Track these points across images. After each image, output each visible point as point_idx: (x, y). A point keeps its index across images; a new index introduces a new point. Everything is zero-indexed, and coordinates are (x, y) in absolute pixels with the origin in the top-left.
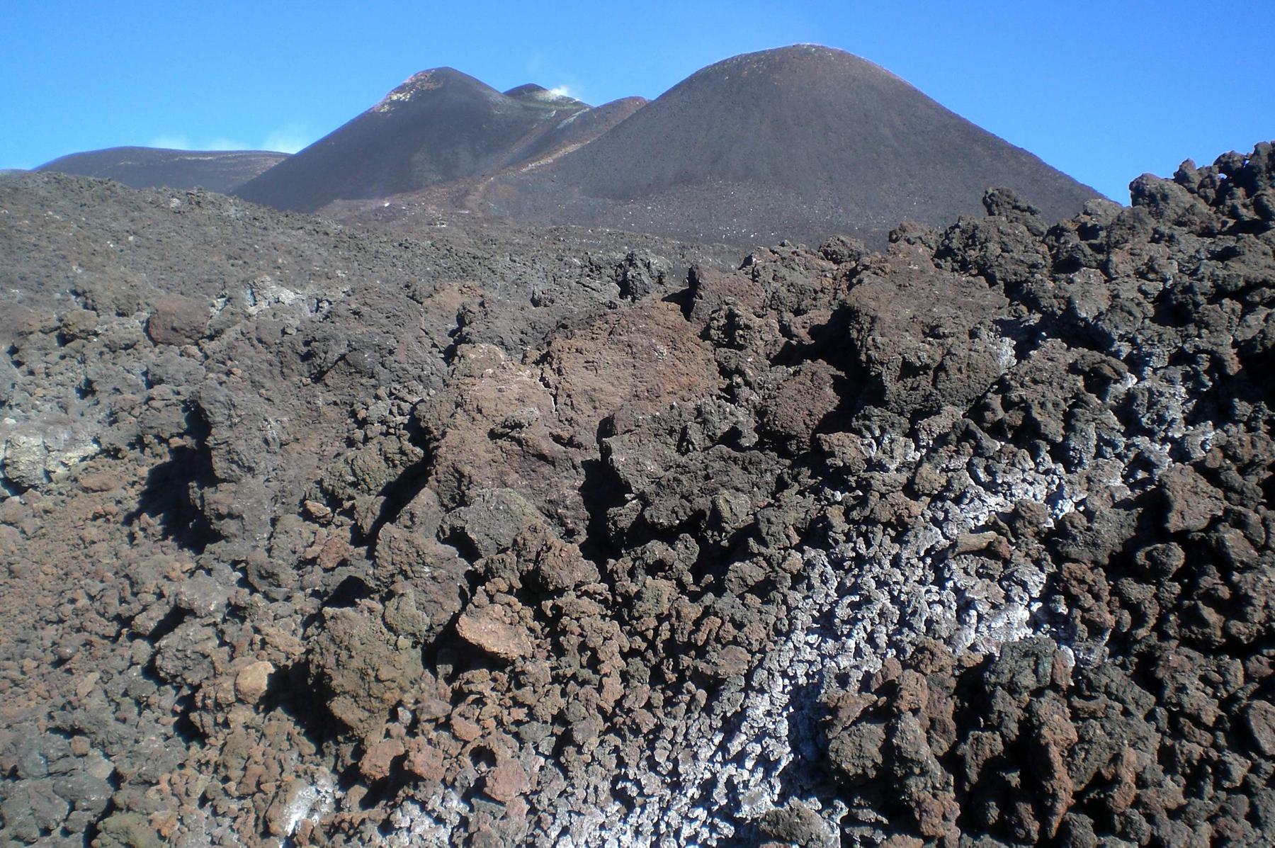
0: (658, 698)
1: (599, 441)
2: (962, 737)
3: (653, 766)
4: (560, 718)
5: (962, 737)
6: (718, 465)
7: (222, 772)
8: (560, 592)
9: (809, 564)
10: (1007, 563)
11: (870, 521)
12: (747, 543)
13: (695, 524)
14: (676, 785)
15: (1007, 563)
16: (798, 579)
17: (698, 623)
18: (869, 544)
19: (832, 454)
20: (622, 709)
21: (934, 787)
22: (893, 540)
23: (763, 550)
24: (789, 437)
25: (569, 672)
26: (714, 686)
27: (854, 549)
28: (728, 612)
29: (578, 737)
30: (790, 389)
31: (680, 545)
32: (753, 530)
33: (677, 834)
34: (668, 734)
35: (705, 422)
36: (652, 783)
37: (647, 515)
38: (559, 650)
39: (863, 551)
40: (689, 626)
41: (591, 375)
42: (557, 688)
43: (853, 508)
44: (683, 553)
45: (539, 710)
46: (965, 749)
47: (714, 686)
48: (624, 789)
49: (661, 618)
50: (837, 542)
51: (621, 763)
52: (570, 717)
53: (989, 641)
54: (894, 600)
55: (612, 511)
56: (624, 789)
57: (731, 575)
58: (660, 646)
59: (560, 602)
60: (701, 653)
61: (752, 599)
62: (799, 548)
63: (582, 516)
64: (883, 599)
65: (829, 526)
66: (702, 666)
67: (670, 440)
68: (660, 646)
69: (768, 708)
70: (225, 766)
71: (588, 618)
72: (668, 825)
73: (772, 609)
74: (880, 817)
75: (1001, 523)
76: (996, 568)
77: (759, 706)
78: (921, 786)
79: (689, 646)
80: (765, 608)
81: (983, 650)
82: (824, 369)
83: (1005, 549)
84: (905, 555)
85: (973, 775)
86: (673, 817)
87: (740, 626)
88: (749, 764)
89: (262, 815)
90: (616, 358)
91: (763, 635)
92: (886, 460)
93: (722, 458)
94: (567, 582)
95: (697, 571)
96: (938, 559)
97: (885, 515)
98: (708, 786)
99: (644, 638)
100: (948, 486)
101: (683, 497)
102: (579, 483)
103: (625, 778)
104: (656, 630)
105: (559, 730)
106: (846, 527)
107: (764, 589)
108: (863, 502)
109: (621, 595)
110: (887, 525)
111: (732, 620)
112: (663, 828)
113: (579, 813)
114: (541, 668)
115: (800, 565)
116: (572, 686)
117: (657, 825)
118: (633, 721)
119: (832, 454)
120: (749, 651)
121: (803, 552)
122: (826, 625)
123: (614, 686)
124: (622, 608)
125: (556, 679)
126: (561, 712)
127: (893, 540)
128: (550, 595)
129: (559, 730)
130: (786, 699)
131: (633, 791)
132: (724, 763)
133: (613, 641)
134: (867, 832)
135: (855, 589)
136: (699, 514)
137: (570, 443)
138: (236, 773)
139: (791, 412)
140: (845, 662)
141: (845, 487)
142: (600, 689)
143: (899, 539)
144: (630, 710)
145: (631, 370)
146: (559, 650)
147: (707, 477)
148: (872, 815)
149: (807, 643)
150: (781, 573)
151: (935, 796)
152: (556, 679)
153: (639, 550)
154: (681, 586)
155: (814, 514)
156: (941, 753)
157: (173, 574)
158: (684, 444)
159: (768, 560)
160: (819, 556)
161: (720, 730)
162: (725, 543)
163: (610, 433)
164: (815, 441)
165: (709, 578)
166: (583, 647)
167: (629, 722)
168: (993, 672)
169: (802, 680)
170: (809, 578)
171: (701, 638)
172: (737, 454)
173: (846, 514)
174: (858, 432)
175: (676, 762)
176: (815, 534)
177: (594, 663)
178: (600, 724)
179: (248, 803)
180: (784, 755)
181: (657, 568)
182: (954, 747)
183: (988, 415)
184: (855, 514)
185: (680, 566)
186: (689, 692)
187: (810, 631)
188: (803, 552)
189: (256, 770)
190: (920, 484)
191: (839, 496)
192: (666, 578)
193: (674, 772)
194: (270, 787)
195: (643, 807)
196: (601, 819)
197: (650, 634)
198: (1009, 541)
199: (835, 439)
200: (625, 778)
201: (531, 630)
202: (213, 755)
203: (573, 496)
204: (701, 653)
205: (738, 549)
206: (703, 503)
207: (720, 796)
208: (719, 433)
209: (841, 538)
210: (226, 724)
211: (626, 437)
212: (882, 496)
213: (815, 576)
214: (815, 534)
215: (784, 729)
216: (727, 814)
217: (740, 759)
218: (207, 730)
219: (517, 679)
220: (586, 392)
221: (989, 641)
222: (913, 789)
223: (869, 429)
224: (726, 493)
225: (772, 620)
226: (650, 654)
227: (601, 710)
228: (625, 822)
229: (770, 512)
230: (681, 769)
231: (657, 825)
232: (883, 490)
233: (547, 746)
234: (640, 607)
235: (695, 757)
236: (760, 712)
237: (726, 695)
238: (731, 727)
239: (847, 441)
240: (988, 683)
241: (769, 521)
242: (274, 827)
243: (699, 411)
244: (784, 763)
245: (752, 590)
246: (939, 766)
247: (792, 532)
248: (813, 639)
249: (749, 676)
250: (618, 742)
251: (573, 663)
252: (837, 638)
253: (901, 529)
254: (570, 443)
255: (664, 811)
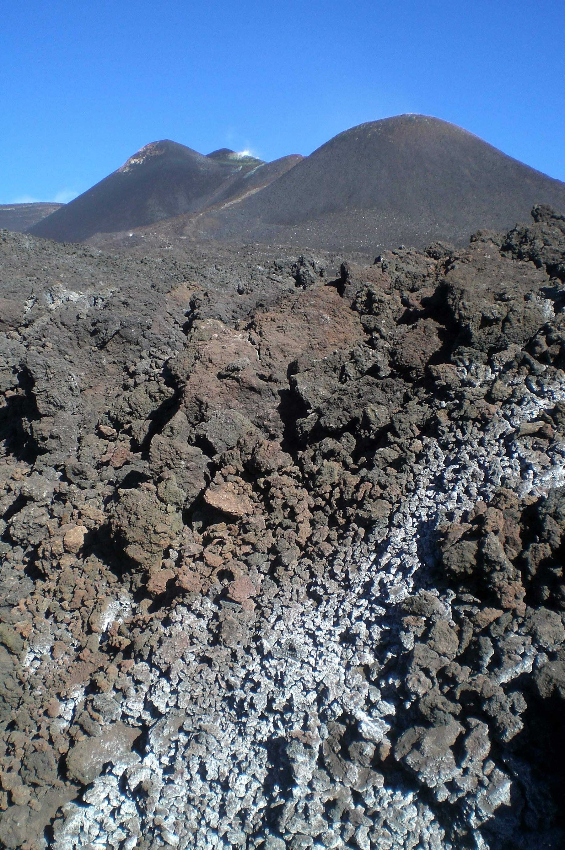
0: (334, 534)
1: (289, 377)
2: (526, 547)
3: (333, 576)
4: (273, 550)
5: (526, 547)
6: (366, 388)
7: (59, 595)
8: (269, 472)
9: (427, 447)
10: (551, 440)
11: (465, 418)
12: (387, 435)
13: (352, 426)
14: (348, 586)
15: (551, 440)
16: (420, 456)
17: (357, 487)
18: (464, 433)
19: (439, 378)
20: (311, 543)
21: (509, 579)
22: (479, 429)
23: (397, 439)
24: (411, 368)
25: (277, 522)
26: (369, 525)
27: (454, 436)
28: (376, 479)
29: (285, 560)
30: (411, 337)
31: (344, 440)
32: (390, 428)
33: (350, 615)
34: (342, 556)
35: (356, 362)
36: (333, 586)
37: (322, 422)
38: (270, 509)
39: (460, 437)
40: (352, 489)
41: (281, 335)
42: (270, 532)
43: (453, 410)
44: (346, 445)
45: (260, 546)
46: (528, 554)
47: (369, 525)
48: (315, 591)
49: (333, 486)
50: (443, 432)
51: (312, 575)
52: (279, 549)
53: (541, 489)
54: (481, 466)
55: (299, 421)
56: (315, 591)
57: (377, 456)
58: (334, 502)
59: (269, 479)
60: (360, 505)
61: (392, 471)
62: (420, 438)
63: (279, 426)
64: (474, 466)
65: (439, 423)
66: (361, 513)
67: (334, 375)
68: (334, 502)
69: (404, 536)
70: (61, 592)
71: (287, 488)
72: (344, 610)
73: (404, 476)
74: (475, 599)
75: (547, 416)
76: (545, 444)
77: (398, 535)
78: (501, 577)
79: (353, 501)
80: (399, 475)
81: (538, 494)
82: (432, 324)
83: (549, 431)
84: (487, 438)
85: (533, 570)
86: (347, 606)
87: (384, 487)
88: (393, 571)
89: (86, 620)
90: (297, 324)
91: (399, 492)
92: (473, 379)
93: (368, 384)
94: (273, 466)
95: (355, 456)
96: (508, 440)
97: (474, 414)
98: (368, 586)
99: (324, 499)
100: (513, 395)
101: (344, 409)
102: (277, 405)
103: (316, 584)
104: (331, 493)
105: (272, 557)
106: (449, 423)
107: (398, 464)
108: (459, 407)
109: (307, 473)
110: (475, 420)
111: (379, 484)
112: (341, 612)
113: (287, 607)
114: (259, 520)
115: (420, 448)
116: (279, 530)
117: (337, 611)
118: (319, 549)
119: (439, 378)
120: (391, 503)
121: (422, 440)
122: (438, 484)
123: (306, 529)
124: (308, 481)
125: (269, 527)
126: (273, 546)
127: (479, 429)
128: (262, 475)
129: (272, 557)
130: (415, 530)
131: (321, 592)
132: (377, 571)
133: (304, 501)
134: (468, 608)
135: (456, 461)
136: (355, 420)
137: (270, 379)
138: (68, 596)
139: (411, 352)
140: (451, 506)
141: (448, 398)
142: (297, 531)
143: (483, 429)
144: (317, 543)
145: (307, 331)
146: (270, 509)
147: (359, 396)
148: (471, 598)
149: (426, 496)
150: (409, 453)
151: (509, 584)
152: (269, 527)
153: (317, 445)
154: (346, 466)
155: (428, 416)
156: (512, 558)
157: (16, 476)
158: (343, 376)
159: (400, 446)
160: (433, 442)
161: (374, 552)
162: (372, 437)
163: (295, 372)
164: (427, 370)
165: (363, 459)
166: (285, 506)
167: (316, 550)
168: (544, 507)
169: (425, 519)
170: (426, 455)
171: (360, 496)
172: (378, 381)
173: (449, 414)
174: (455, 363)
175: (347, 573)
176: (429, 428)
177: (293, 515)
178: (298, 552)
179: (77, 613)
180: (415, 564)
181: (330, 455)
182: (521, 554)
183: (538, 349)
184: (455, 414)
185: (345, 453)
186: (354, 529)
187: (428, 488)
188: (422, 440)
189: (80, 593)
190: (496, 394)
191: (444, 404)
192: (335, 461)
193: (347, 579)
194: (90, 603)
195: (328, 601)
196: (302, 609)
197: (327, 496)
198: (553, 427)
199: (441, 367)
200: (316, 584)
201: (251, 497)
202: (52, 585)
203: (273, 413)
204: (360, 505)
205: (382, 439)
206: (357, 413)
207: (376, 591)
208: (366, 369)
209: (446, 430)
210: (59, 567)
211: (306, 374)
212: (472, 402)
213: (430, 454)
214: (429, 428)
215: (414, 548)
216: (380, 602)
217: (387, 568)
218: (47, 571)
219: (244, 528)
220: (278, 346)
221: (541, 489)
222: (496, 580)
223: (462, 361)
224: (372, 406)
225: (404, 483)
226: (328, 508)
227: (298, 543)
228: (317, 610)
229: (401, 416)
230: (350, 577)
231: (337, 611)
232: (472, 398)
233: (265, 567)
234: (320, 479)
235: (359, 569)
236: (399, 539)
237: (377, 530)
238: (380, 549)
239: (448, 370)
240: (541, 514)
241: (400, 421)
242: (94, 627)
243: (352, 355)
244: (415, 569)
245: (391, 465)
246: (512, 565)
247: (415, 428)
248: (430, 493)
249: (391, 518)
250: (310, 562)
251: (279, 516)
252: (445, 492)
253: (484, 422)
254: (270, 379)
255: (341, 602)
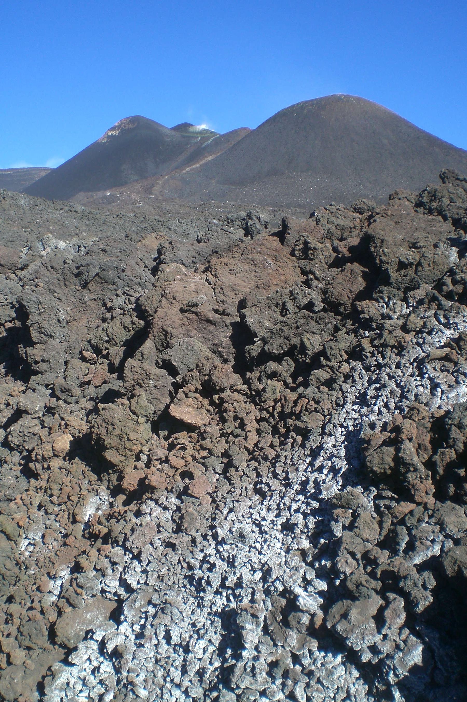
55: (248, 347)
63: (231, 352)
94: (226, 385)
102: (229, 334)
203: (226, 341)
